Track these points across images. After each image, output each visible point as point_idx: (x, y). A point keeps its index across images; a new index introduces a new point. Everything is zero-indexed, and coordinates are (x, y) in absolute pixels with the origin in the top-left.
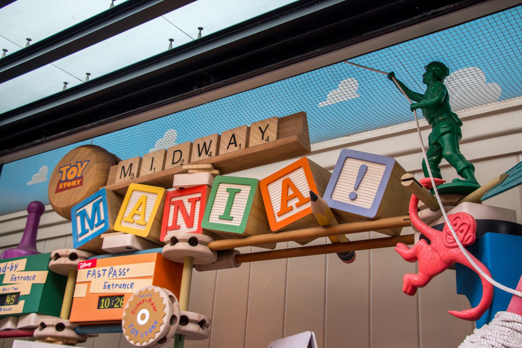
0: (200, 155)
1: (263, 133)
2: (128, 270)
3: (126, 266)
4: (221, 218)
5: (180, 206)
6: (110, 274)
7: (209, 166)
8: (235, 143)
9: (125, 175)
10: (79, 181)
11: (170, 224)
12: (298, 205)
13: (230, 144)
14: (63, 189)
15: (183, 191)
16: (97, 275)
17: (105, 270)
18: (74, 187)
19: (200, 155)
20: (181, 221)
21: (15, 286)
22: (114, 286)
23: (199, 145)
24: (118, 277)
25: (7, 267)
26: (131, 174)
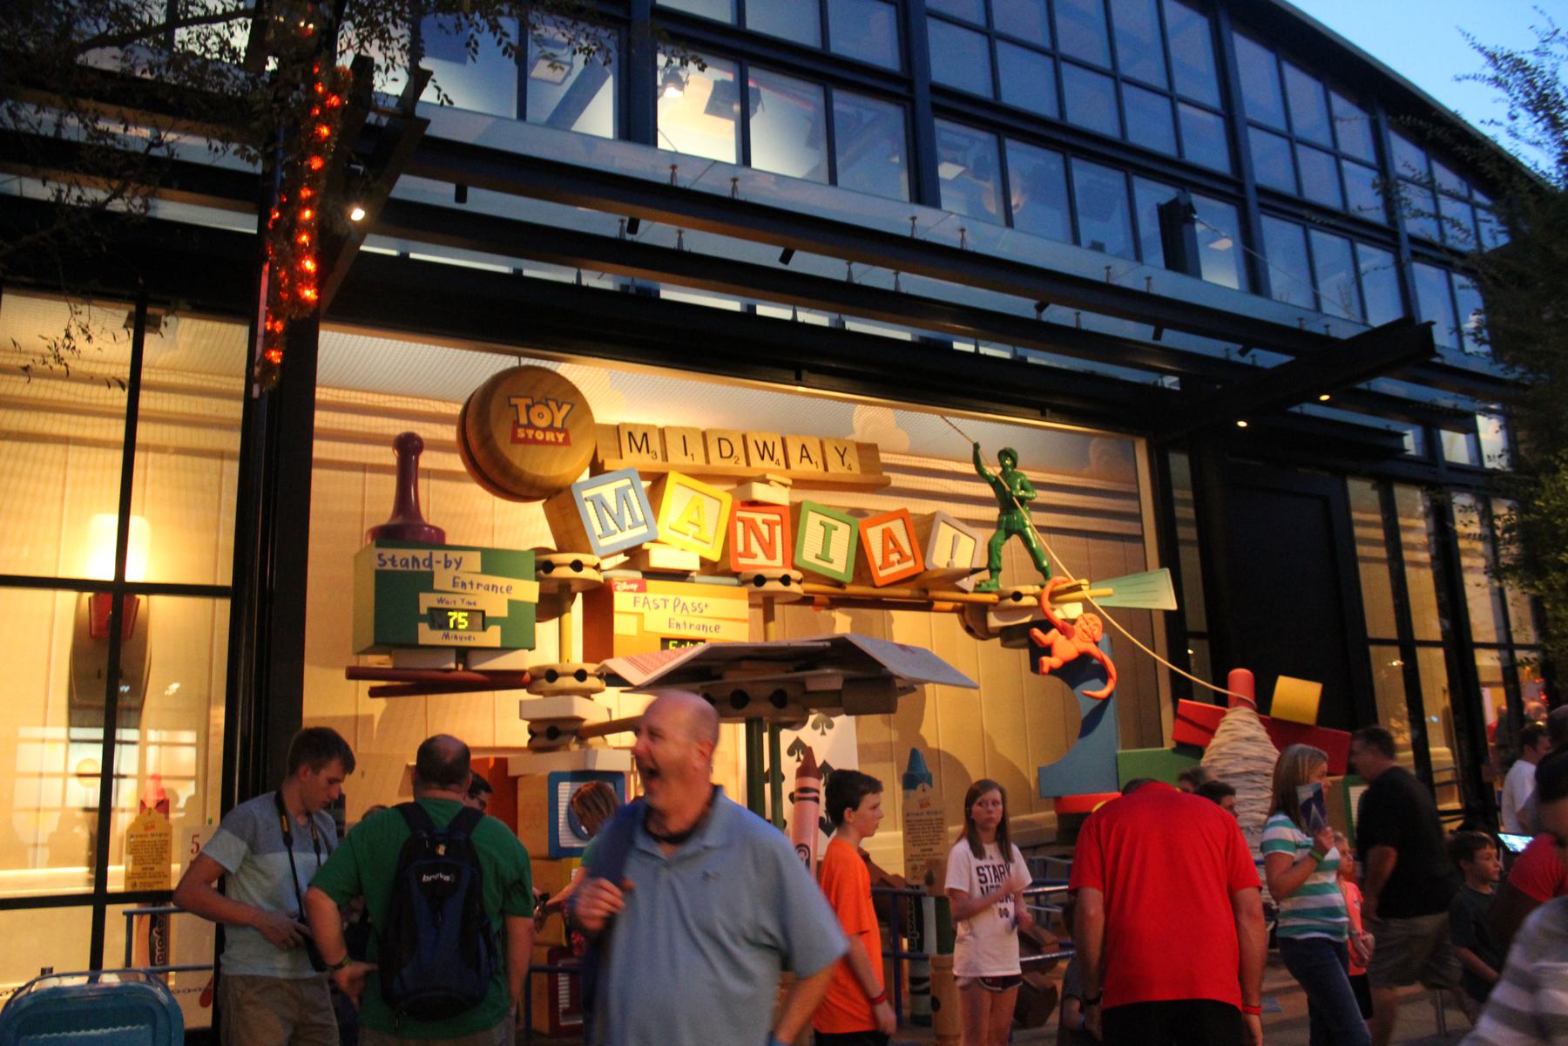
0: (762, 458)
1: (842, 457)
3: (704, 600)
4: (817, 557)
5: (750, 526)
6: (675, 607)
7: (790, 482)
8: (808, 456)
9: (640, 450)
10: (561, 437)
11: (740, 548)
12: (899, 562)
13: (802, 457)
14: (526, 441)
15: (754, 504)
16: (652, 606)
19: (762, 458)
20: (755, 547)
21: (472, 599)
23: (756, 442)
24: (691, 613)
25: (434, 559)
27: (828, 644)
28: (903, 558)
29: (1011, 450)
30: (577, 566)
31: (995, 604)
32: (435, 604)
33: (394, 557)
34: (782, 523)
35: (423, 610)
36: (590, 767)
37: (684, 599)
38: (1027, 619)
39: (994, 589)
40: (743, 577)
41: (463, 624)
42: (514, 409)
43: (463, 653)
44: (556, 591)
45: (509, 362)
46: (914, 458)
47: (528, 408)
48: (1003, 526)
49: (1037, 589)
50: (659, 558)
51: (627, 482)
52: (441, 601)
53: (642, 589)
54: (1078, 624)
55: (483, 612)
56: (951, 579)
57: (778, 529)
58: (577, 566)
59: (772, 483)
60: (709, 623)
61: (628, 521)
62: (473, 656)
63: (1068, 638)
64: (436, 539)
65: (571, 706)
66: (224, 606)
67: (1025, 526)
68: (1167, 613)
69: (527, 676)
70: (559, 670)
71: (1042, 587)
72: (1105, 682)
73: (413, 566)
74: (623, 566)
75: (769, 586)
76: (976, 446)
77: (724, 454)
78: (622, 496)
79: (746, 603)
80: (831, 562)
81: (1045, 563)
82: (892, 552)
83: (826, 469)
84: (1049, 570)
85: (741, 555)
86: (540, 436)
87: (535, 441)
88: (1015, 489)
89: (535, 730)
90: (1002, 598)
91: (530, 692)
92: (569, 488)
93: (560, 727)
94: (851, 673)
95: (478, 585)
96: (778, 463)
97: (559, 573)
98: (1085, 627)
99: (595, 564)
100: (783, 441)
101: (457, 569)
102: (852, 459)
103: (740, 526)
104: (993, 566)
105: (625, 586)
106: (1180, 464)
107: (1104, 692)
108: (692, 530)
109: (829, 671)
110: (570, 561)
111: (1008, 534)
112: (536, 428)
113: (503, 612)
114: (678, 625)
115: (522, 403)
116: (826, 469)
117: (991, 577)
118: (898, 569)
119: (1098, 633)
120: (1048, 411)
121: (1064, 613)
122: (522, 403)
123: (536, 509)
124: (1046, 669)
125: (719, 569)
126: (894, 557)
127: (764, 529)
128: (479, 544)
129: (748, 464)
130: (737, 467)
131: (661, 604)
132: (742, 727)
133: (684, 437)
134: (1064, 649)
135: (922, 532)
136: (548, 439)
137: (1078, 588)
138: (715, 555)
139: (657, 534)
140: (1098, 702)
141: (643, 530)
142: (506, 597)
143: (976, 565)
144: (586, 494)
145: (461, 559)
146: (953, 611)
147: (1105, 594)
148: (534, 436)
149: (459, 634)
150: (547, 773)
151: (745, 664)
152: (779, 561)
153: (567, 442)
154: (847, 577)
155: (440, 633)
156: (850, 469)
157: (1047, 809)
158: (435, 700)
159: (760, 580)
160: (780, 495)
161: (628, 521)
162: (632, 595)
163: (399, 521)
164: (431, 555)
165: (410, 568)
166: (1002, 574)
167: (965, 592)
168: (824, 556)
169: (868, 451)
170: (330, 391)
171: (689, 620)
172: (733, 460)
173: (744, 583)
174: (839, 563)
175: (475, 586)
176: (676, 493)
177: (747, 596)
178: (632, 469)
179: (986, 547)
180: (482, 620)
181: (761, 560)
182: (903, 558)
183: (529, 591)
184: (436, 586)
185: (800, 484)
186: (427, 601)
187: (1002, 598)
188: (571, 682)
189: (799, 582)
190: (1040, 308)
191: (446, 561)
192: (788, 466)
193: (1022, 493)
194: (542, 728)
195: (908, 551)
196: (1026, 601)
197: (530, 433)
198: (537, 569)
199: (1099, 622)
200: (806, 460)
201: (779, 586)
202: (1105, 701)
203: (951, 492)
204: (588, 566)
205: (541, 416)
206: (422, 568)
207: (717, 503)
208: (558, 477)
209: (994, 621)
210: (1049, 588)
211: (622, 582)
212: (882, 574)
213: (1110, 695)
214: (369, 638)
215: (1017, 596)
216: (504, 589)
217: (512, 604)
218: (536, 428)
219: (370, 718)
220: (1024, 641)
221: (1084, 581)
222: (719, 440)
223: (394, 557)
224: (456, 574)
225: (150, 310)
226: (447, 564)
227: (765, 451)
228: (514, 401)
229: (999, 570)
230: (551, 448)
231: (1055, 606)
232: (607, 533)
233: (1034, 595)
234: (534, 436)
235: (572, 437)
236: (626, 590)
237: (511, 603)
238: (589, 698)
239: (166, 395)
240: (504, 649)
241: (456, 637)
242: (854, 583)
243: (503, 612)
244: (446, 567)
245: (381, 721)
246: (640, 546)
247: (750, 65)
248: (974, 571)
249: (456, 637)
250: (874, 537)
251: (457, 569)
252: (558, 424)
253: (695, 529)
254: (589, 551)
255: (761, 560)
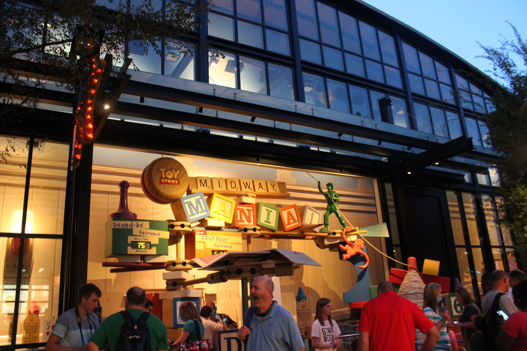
0: (246, 188)
1: (273, 187)
2: (227, 239)
3: (226, 237)
5: (242, 211)
7: (255, 196)
8: (262, 187)
9: (204, 186)
10: (177, 182)
11: (239, 219)
12: (293, 223)
13: (259, 187)
15: (243, 204)
16: (209, 239)
17: (213, 237)
18: (173, 184)
19: (246, 188)
20: (244, 218)
21: (146, 238)
22: (221, 246)
24: (222, 242)
26: (207, 186)
27: (269, 252)
28: (295, 221)
29: (331, 183)
30: (182, 226)
31: (327, 237)
32: (134, 240)
33: (119, 224)
34: (253, 210)
35: (129, 242)
36: (188, 296)
37: (219, 237)
38: (338, 241)
39: (326, 231)
40: (240, 229)
41: (143, 246)
42: (160, 172)
43: (143, 257)
44: (175, 234)
45: (159, 156)
46: (298, 187)
47: (165, 172)
48: (329, 210)
49: (341, 231)
50: (211, 223)
51: (199, 197)
52: (135, 239)
53: (205, 234)
54: (355, 243)
55: (150, 242)
56: (311, 228)
57: (252, 212)
58: (182, 226)
59: (249, 196)
60: (228, 245)
61: (200, 210)
62: (147, 258)
63: (352, 248)
64: (133, 217)
65: (181, 274)
66: (60, 242)
67: (336, 209)
68: (386, 238)
69: (165, 264)
70: (176, 262)
71: (343, 230)
72: (365, 262)
73: (126, 227)
74: (199, 226)
75: (249, 232)
76: (319, 182)
77: (233, 187)
78: (198, 201)
79: (241, 238)
80: (270, 223)
81: (344, 222)
82: (291, 219)
83: (268, 191)
84: (345, 224)
85: (239, 221)
86: (169, 181)
87: (167, 183)
88: (333, 197)
89: (168, 283)
90: (329, 234)
91: (166, 270)
92: (180, 199)
93: (177, 282)
94: (277, 262)
95: (148, 233)
96: (251, 189)
97: (176, 228)
98: (358, 244)
99: (189, 225)
100: (253, 182)
101: (141, 227)
102: (277, 187)
103: (238, 211)
104: (326, 223)
105: (199, 233)
106: (388, 187)
107: (365, 266)
108: (222, 213)
109: (270, 261)
110: (180, 224)
111: (331, 212)
112: (168, 179)
113: (157, 242)
114: (218, 246)
115: (163, 170)
116: (268, 191)
117: (325, 227)
118: (293, 225)
119: (362, 246)
120: (343, 170)
121: (350, 239)
122: (163, 170)
123: (168, 206)
124: (345, 258)
125: (232, 226)
126: (292, 221)
127: (247, 212)
128: (148, 219)
129: (241, 190)
130: (237, 191)
131: (212, 238)
132: (240, 281)
133: (219, 181)
134: (351, 251)
135: (301, 212)
136: (172, 182)
137: (355, 230)
138: (230, 222)
139: (210, 215)
140: (363, 270)
141: (205, 213)
142: (158, 237)
143: (320, 223)
144: (185, 201)
145: (142, 224)
146: (312, 239)
147: (364, 232)
148: (167, 181)
149: (141, 250)
150: (173, 298)
151: (241, 259)
152: (252, 223)
153: (179, 183)
154: (276, 229)
155: (135, 250)
156: (277, 191)
157: (347, 307)
158: (133, 273)
159: (246, 230)
160: (251, 200)
161: (200, 210)
162: (202, 236)
163: (121, 211)
164: (132, 223)
165: (125, 228)
166: (329, 226)
167: (316, 232)
168: (268, 221)
169: (282, 185)
170: (97, 167)
171: (221, 244)
172: (236, 189)
173: (240, 231)
174: (273, 223)
175: (147, 233)
176: (216, 200)
177: (241, 235)
178: (201, 192)
179: (323, 217)
180: (149, 245)
181: (246, 223)
182: (295, 221)
183: (166, 235)
184: (134, 234)
185: (259, 196)
186: (130, 239)
187: (329, 234)
188: (181, 266)
189: (259, 230)
190: (340, 135)
191: (137, 225)
192: (255, 190)
193: (335, 198)
194: (171, 283)
195: (296, 219)
196: (337, 235)
197: (166, 180)
198: (169, 227)
199: (362, 241)
200: (261, 188)
201: (252, 232)
202: (365, 269)
203: (311, 198)
204: (186, 226)
205: (170, 174)
206: (129, 228)
207: (231, 204)
208: (176, 195)
209: (326, 242)
210: (345, 230)
211: (198, 231)
212: (288, 227)
213: (367, 267)
214: (110, 252)
215: (334, 233)
216: (157, 235)
217: (160, 239)
218: (168, 179)
219: (111, 280)
220: (337, 249)
221: (357, 228)
222: (231, 182)
223: (119, 224)
224: (141, 229)
225: (35, 140)
226: (138, 226)
227: (247, 185)
228: (160, 170)
229: (328, 225)
230: (173, 185)
231: (347, 237)
232: (193, 214)
233: (340, 233)
234: (167, 181)
235: (180, 182)
236: (199, 234)
237: (160, 239)
238: (187, 272)
239: (40, 168)
240: (158, 255)
241: (141, 251)
242: (278, 230)
243: (157, 242)
244: (137, 227)
245: (114, 281)
246: (204, 219)
247: (240, 55)
248: (319, 225)
249: (141, 251)
250: (285, 214)
251: (141, 227)
252: (176, 177)
253: (223, 212)
254: (187, 221)
255: (246, 223)
